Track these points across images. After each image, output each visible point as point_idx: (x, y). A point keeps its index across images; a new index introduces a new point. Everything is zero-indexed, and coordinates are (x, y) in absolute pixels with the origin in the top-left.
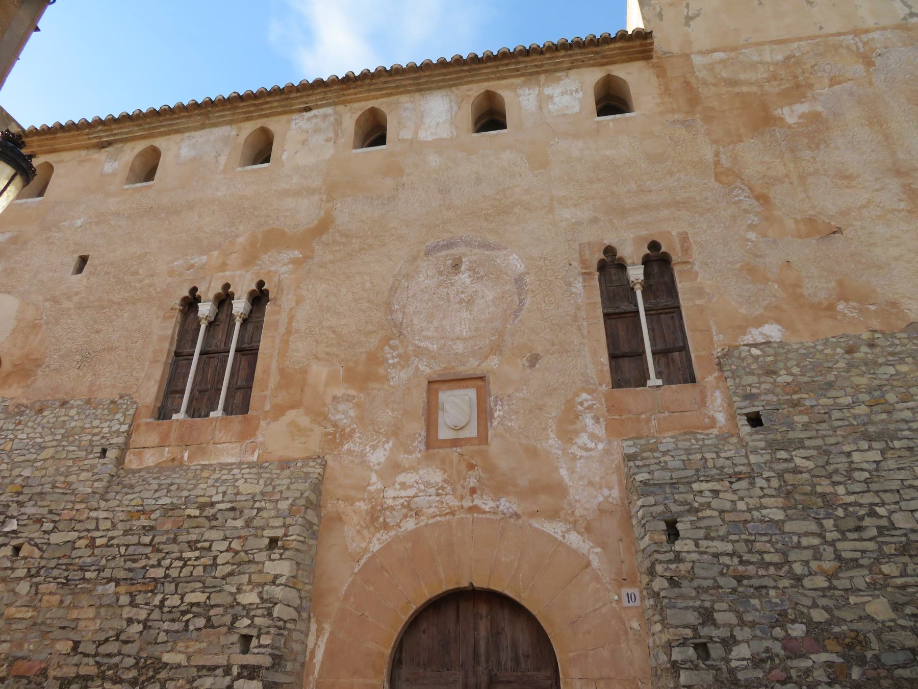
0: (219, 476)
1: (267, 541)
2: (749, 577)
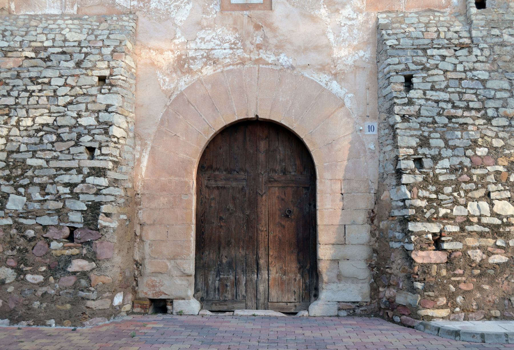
0: (46, 25)
1: (97, 79)
2: (457, 117)
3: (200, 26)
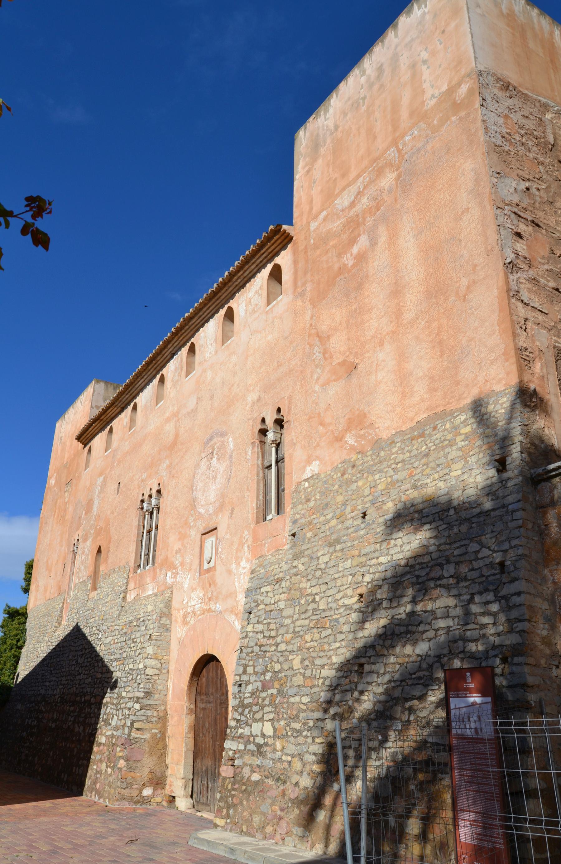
3: (193, 589)
